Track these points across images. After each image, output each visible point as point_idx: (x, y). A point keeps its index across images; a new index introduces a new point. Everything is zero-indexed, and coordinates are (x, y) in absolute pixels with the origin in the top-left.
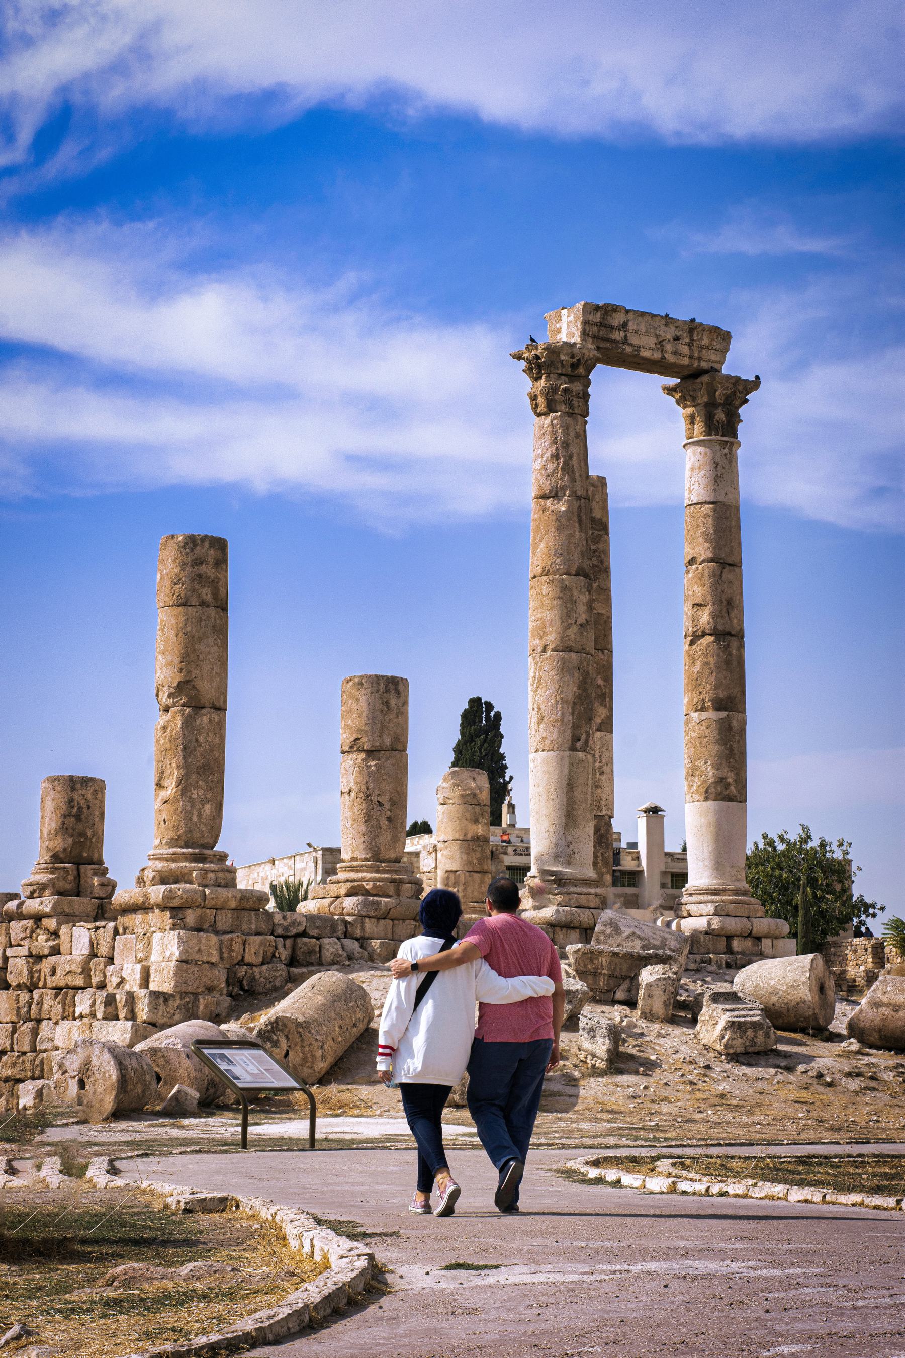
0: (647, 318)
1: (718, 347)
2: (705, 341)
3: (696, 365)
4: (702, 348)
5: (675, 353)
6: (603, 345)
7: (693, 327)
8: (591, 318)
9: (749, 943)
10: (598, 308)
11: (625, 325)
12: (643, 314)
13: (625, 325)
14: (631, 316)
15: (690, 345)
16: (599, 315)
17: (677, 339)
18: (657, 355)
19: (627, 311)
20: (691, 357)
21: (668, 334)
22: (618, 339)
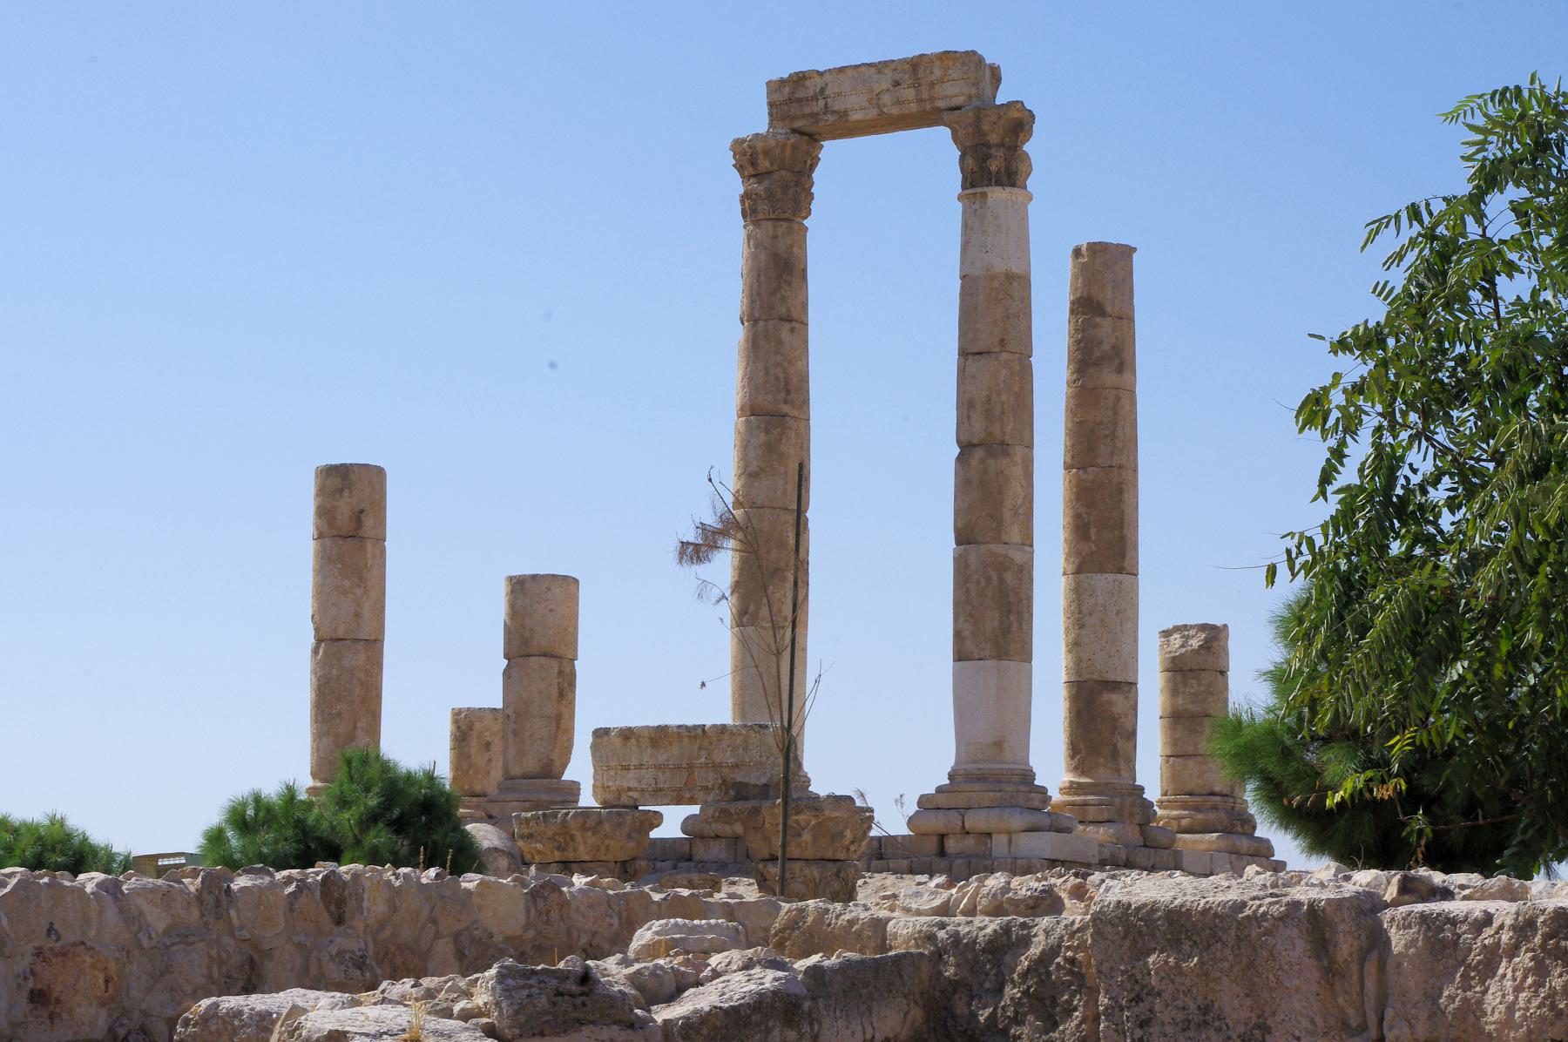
0: (850, 73)
1: (955, 76)
2: (937, 73)
3: (928, 107)
4: (932, 85)
5: (899, 102)
6: (798, 124)
7: (916, 65)
8: (778, 97)
9: (970, 842)
10: (782, 82)
11: (823, 90)
12: (842, 70)
13: (823, 90)
14: (827, 77)
15: (917, 85)
16: (787, 90)
17: (897, 84)
18: (872, 113)
19: (820, 74)
20: (921, 101)
21: (886, 85)
22: (816, 110)
